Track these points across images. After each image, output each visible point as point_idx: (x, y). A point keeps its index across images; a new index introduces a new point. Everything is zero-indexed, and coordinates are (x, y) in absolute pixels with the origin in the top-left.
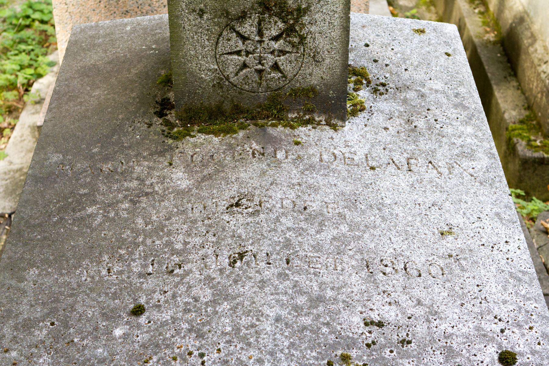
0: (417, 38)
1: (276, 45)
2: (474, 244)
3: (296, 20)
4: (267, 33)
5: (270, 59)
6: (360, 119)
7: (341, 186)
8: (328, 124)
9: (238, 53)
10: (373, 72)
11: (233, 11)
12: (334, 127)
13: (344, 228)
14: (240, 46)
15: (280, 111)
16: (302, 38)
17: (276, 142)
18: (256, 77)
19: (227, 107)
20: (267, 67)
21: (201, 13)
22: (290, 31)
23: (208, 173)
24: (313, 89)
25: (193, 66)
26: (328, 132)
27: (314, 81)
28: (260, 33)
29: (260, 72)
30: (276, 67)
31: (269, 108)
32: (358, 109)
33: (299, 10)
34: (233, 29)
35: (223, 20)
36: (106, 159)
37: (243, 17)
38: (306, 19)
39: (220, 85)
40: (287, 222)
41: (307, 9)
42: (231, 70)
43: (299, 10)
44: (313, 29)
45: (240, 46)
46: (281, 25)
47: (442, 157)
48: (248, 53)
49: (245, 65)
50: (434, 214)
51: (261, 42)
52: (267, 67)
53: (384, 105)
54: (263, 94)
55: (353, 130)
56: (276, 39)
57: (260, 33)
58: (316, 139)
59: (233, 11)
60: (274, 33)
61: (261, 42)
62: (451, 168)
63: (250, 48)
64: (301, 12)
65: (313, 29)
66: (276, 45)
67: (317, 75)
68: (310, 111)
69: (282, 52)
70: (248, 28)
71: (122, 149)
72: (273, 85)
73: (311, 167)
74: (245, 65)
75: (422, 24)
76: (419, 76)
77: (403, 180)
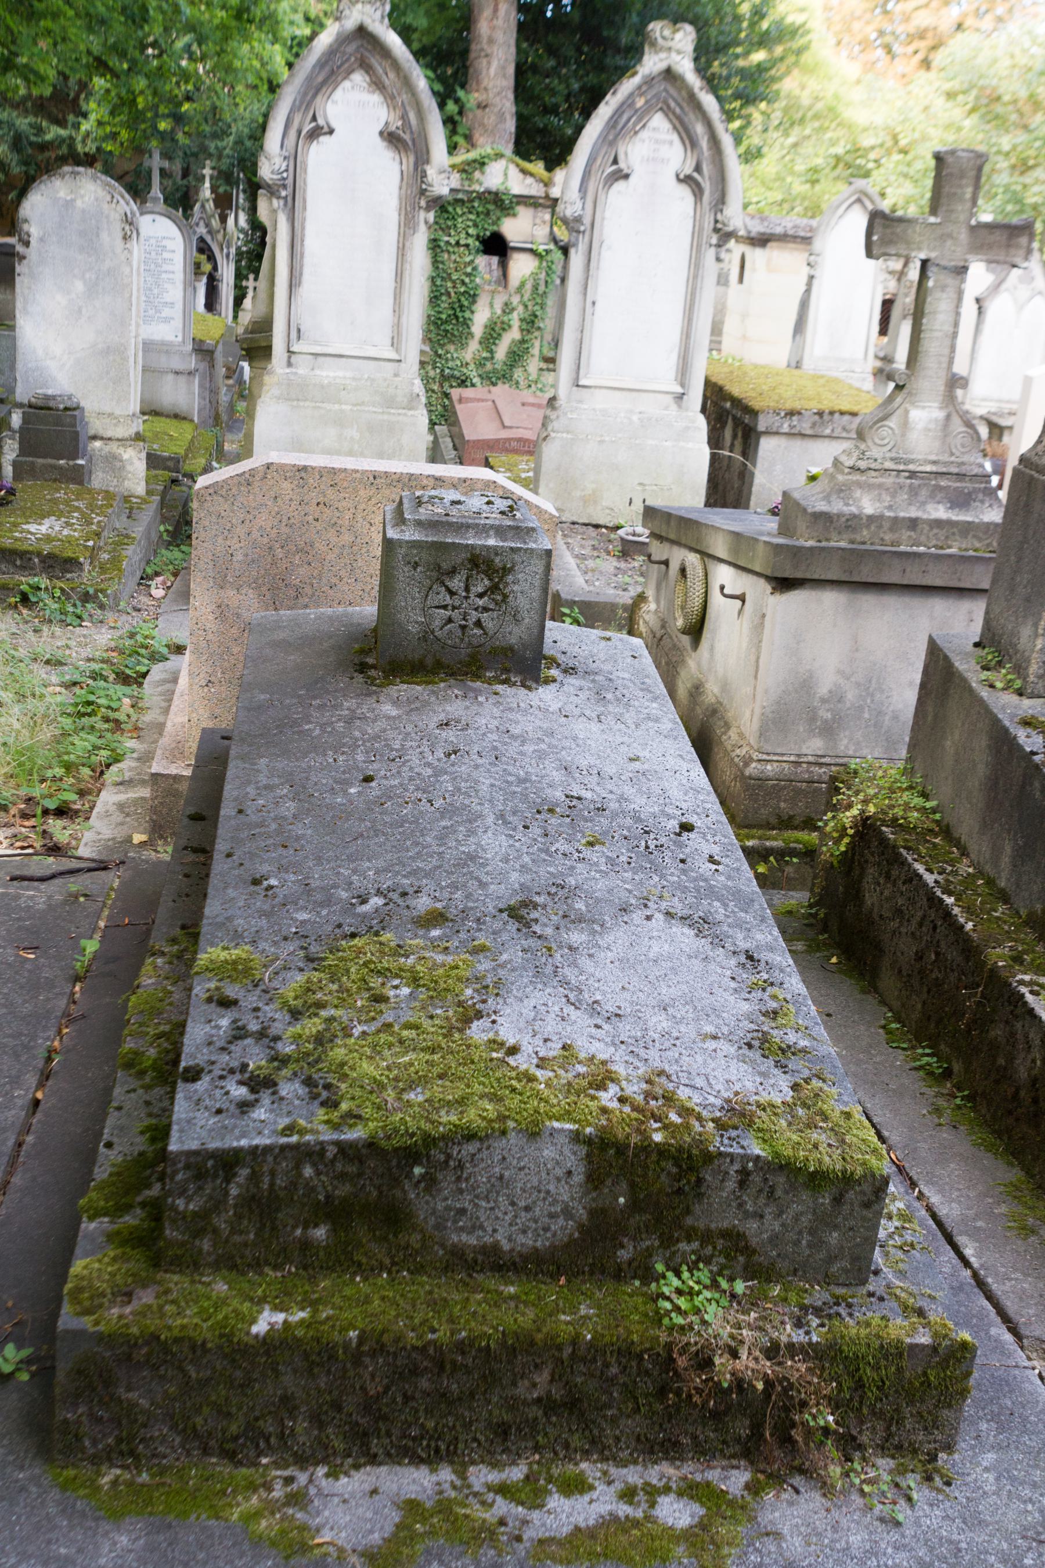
0: (603, 643)
1: (480, 602)
2: (660, 769)
3: (501, 579)
4: (473, 589)
5: (474, 615)
6: (553, 687)
7: (538, 723)
8: (523, 685)
9: (445, 607)
10: (561, 658)
11: (445, 566)
12: (529, 689)
13: (543, 746)
14: (448, 600)
15: (480, 667)
16: (505, 597)
17: (478, 692)
18: (459, 633)
19: (429, 661)
20: (470, 623)
21: (416, 565)
22: (494, 588)
23: (415, 707)
24: (511, 649)
25: (402, 617)
26: (523, 691)
27: (513, 640)
28: (467, 589)
29: (463, 628)
30: (478, 624)
31: (469, 665)
32: (549, 681)
33: (504, 568)
34: (443, 583)
35: (435, 574)
36: (315, 698)
37: (453, 572)
38: (510, 578)
39: (425, 639)
40: (495, 737)
41: (511, 569)
42: (437, 623)
43: (504, 568)
44: (516, 588)
45: (448, 600)
46: (487, 582)
47: (630, 717)
48: (454, 608)
49: (450, 620)
50: (623, 749)
51: (467, 598)
52: (470, 623)
53: (571, 680)
54: (464, 652)
55: (545, 695)
56: (481, 596)
57: (467, 589)
58: (514, 695)
59: (445, 566)
60: (480, 590)
61: (467, 598)
62: (637, 726)
63: (457, 603)
64: (506, 571)
65: (516, 588)
66: (480, 602)
67: (515, 634)
68: (507, 670)
69: (486, 609)
70: (457, 583)
71: (328, 692)
72: (475, 641)
73: (511, 709)
74: (450, 620)
75: (608, 634)
76: (607, 667)
77: (595, 727)
